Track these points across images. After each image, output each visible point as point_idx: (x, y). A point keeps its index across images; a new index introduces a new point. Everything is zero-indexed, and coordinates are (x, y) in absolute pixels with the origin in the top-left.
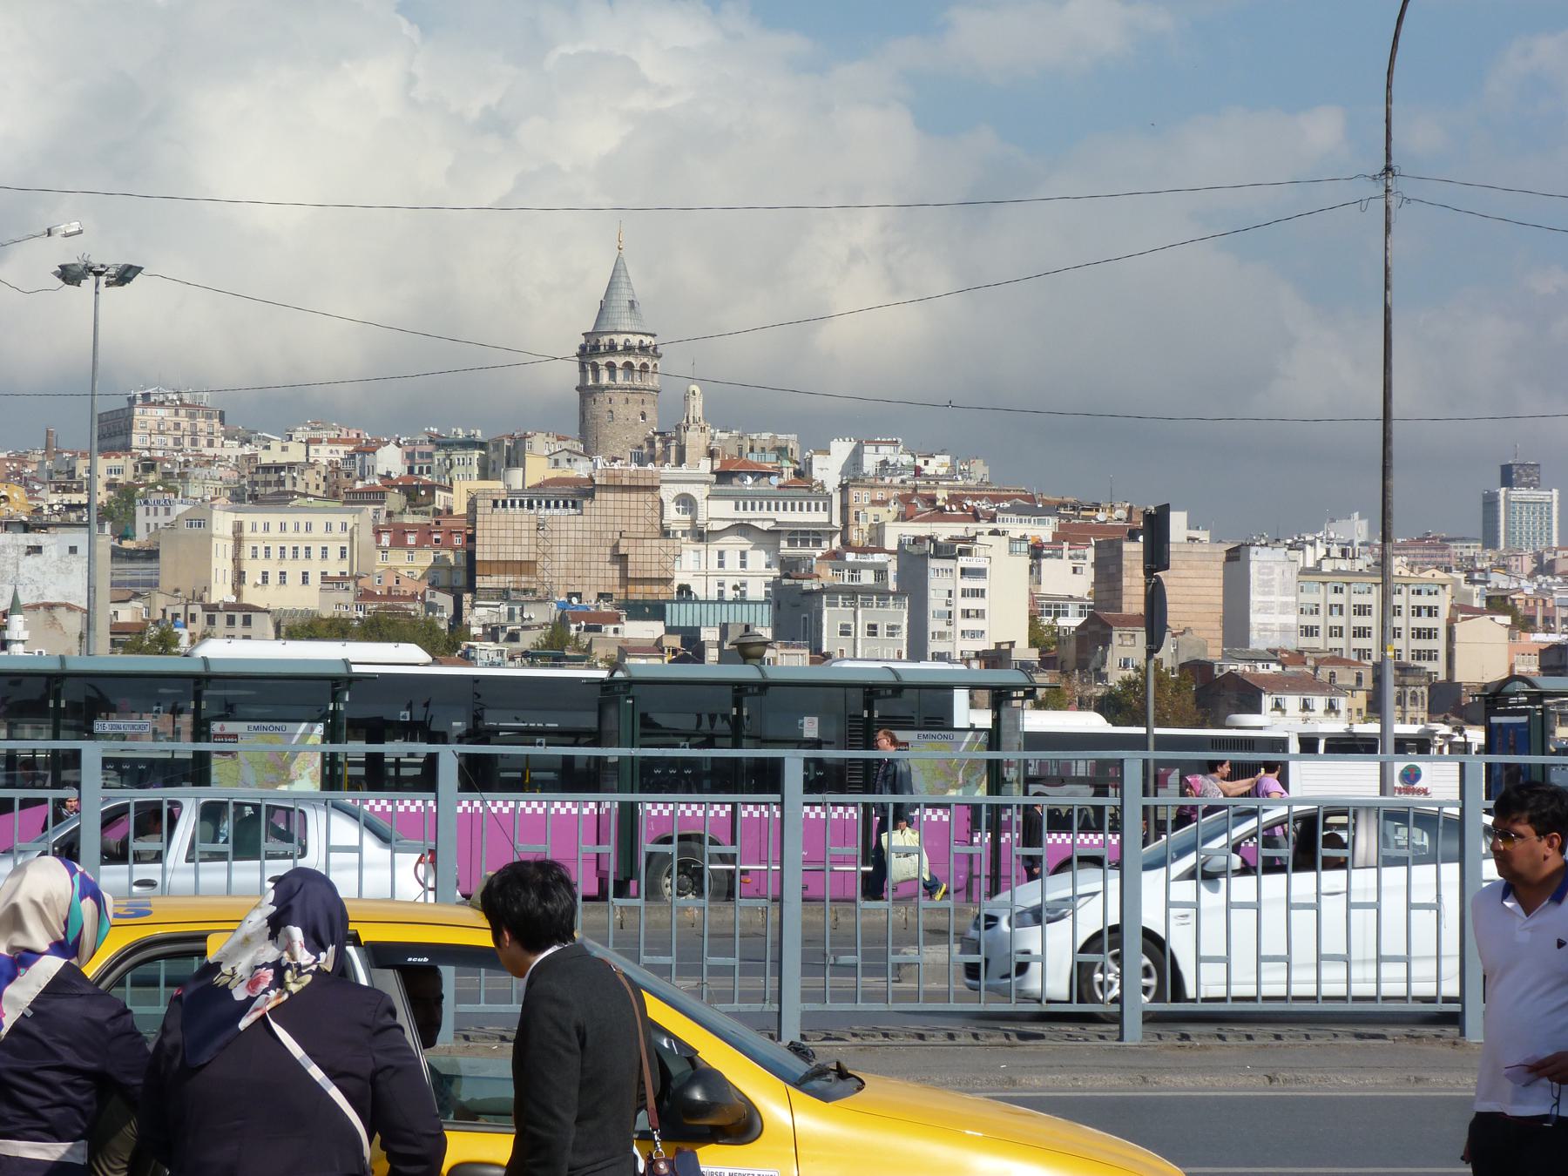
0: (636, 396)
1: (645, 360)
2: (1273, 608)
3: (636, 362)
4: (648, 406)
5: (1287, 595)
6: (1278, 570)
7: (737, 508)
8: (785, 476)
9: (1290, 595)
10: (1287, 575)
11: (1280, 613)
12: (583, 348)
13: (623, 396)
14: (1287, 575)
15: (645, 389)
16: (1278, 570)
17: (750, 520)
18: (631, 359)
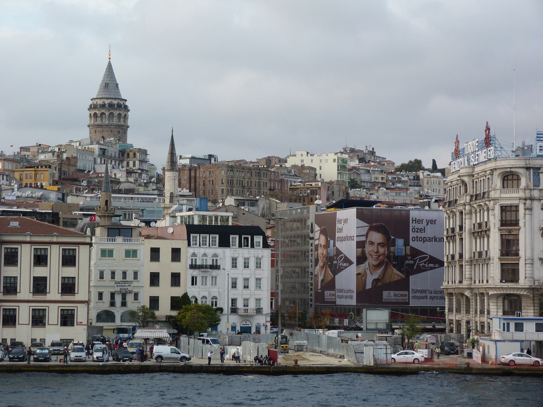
0: (99, 129)
1: (104, 111)
4: (106, 133)
13: (94, 129)
18: (97, 112)
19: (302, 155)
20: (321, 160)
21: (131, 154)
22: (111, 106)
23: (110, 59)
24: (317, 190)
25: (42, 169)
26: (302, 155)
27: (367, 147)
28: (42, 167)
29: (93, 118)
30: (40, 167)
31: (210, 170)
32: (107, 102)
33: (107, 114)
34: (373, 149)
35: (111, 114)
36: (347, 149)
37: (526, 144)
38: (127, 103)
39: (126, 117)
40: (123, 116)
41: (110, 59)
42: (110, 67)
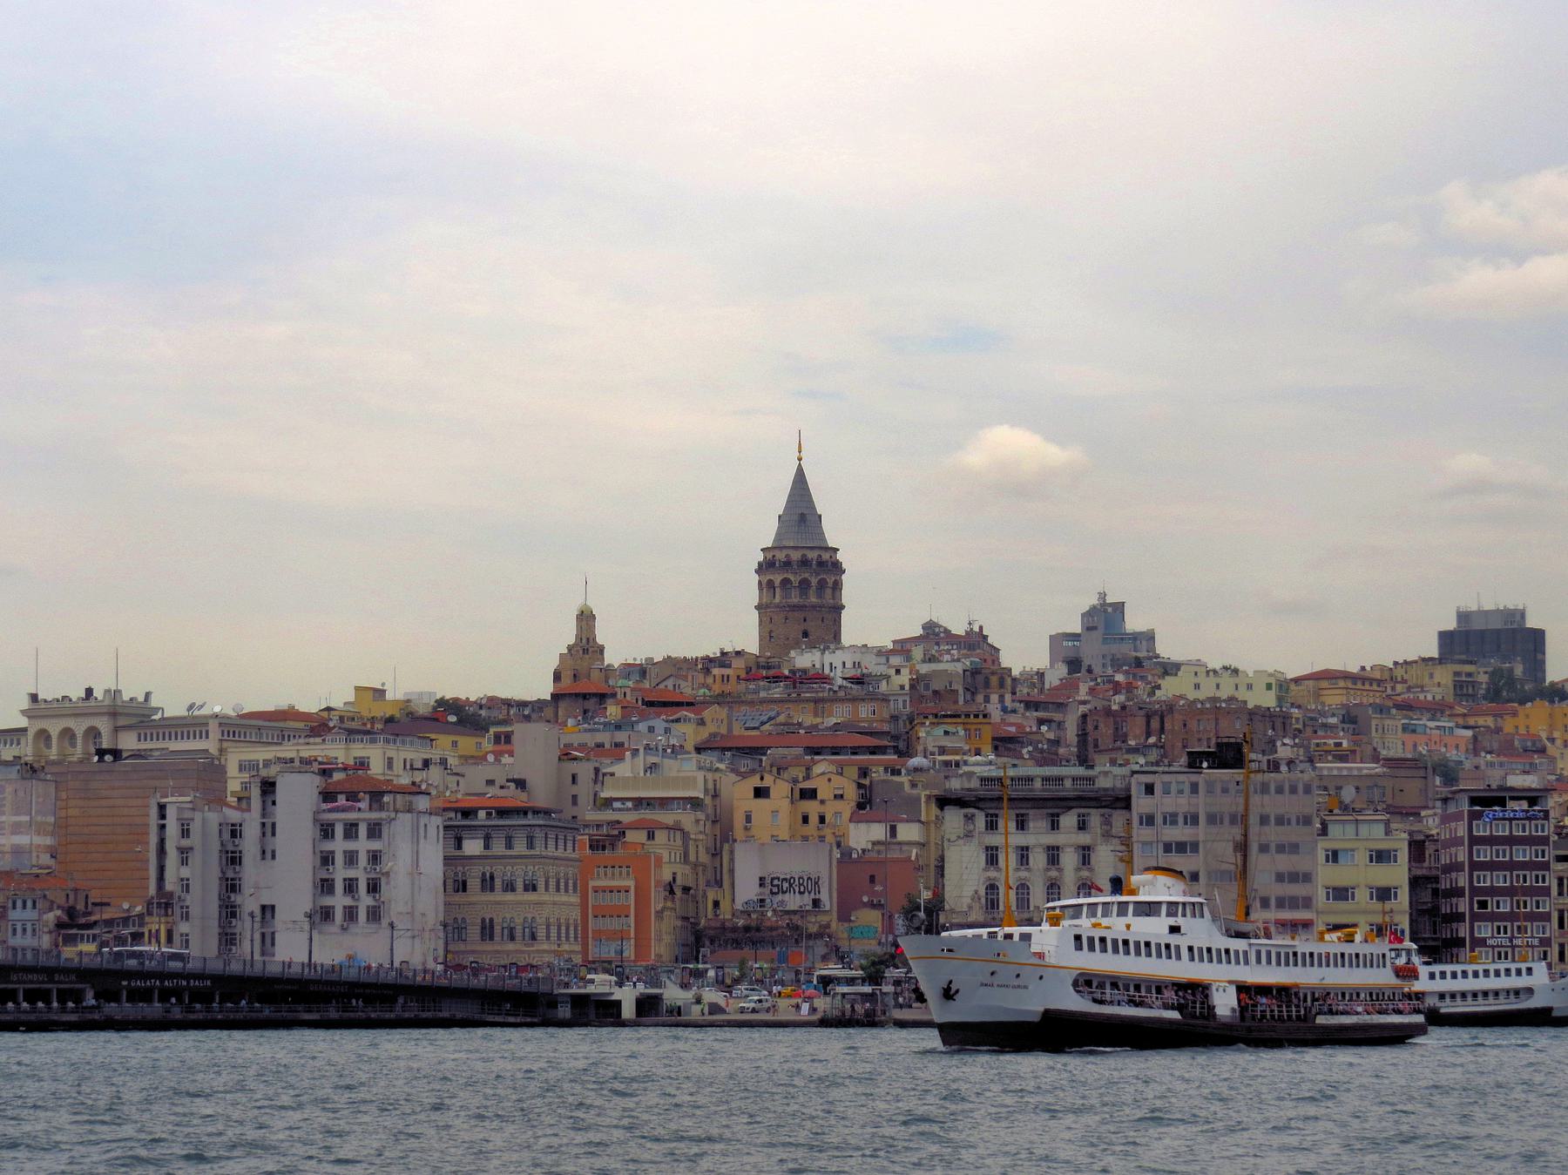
0: (796, 614)
1: (807, 575)
2: (3, 828)
3: (795, 579)
5: (17, 814)
6: (9, 789)
7: (139, 740)
8: (619, 696)
9: (25, 814)
10: (21, 794)
11: (12, 834)
12: (761, 569)
14: (21, 794)
15: (806, 606)
16: (9, 789)
17: (151, 750)
18: (792, 577)
19: (1196, 674)
20: (1237, 686)
21: (994, 680)
22: (804, 562)
23: (800, 459)
24: (1347, 755)
25: (976, 720)
26: (1196, 674)
27: (970, 624)
28: (976, 716)
29: (778, 590)
30: (972, 716)
31: (1199, 717)
32: (796, 556)
33: (814, 581)
34: (981, 628)
35: (822, 584)
36: (937, 630)
37: (1109, 600)
38: (839, 556)
39: (837, 586)
40: (830, 584)
41: (800, 459)
42: (800, 478)
